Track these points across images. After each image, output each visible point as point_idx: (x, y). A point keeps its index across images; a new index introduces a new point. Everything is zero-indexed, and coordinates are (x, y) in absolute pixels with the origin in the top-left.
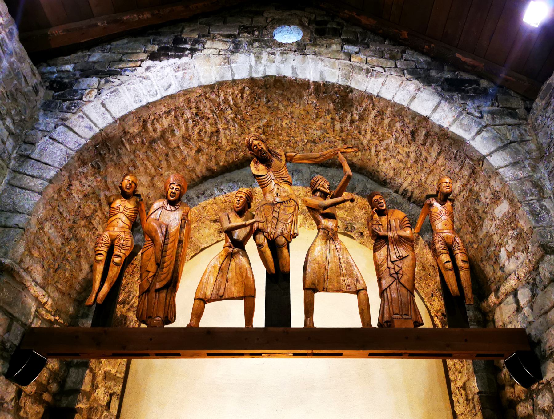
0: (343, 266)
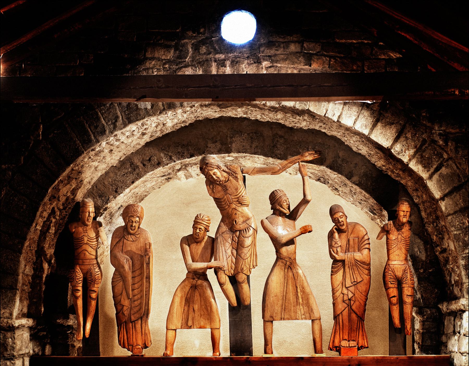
0: (299, 295)
